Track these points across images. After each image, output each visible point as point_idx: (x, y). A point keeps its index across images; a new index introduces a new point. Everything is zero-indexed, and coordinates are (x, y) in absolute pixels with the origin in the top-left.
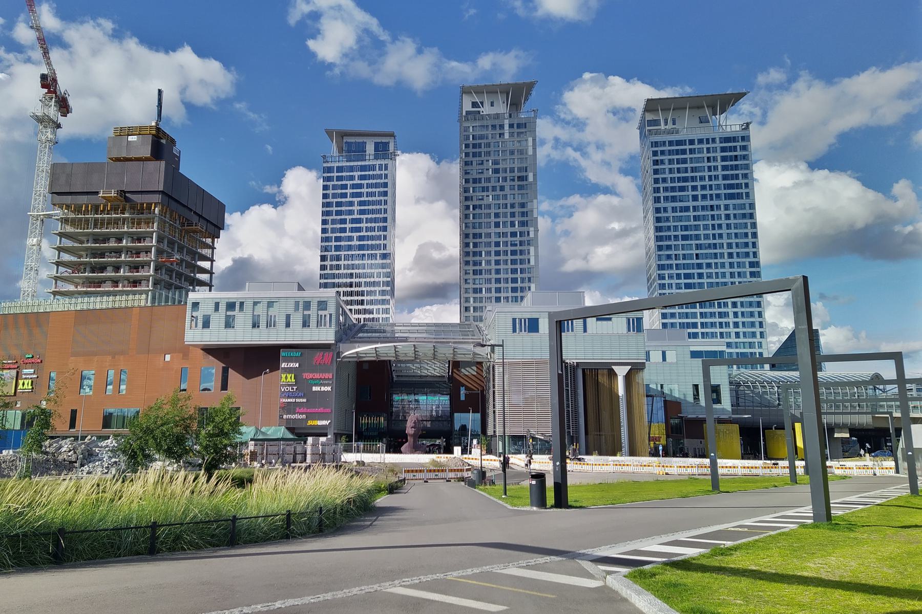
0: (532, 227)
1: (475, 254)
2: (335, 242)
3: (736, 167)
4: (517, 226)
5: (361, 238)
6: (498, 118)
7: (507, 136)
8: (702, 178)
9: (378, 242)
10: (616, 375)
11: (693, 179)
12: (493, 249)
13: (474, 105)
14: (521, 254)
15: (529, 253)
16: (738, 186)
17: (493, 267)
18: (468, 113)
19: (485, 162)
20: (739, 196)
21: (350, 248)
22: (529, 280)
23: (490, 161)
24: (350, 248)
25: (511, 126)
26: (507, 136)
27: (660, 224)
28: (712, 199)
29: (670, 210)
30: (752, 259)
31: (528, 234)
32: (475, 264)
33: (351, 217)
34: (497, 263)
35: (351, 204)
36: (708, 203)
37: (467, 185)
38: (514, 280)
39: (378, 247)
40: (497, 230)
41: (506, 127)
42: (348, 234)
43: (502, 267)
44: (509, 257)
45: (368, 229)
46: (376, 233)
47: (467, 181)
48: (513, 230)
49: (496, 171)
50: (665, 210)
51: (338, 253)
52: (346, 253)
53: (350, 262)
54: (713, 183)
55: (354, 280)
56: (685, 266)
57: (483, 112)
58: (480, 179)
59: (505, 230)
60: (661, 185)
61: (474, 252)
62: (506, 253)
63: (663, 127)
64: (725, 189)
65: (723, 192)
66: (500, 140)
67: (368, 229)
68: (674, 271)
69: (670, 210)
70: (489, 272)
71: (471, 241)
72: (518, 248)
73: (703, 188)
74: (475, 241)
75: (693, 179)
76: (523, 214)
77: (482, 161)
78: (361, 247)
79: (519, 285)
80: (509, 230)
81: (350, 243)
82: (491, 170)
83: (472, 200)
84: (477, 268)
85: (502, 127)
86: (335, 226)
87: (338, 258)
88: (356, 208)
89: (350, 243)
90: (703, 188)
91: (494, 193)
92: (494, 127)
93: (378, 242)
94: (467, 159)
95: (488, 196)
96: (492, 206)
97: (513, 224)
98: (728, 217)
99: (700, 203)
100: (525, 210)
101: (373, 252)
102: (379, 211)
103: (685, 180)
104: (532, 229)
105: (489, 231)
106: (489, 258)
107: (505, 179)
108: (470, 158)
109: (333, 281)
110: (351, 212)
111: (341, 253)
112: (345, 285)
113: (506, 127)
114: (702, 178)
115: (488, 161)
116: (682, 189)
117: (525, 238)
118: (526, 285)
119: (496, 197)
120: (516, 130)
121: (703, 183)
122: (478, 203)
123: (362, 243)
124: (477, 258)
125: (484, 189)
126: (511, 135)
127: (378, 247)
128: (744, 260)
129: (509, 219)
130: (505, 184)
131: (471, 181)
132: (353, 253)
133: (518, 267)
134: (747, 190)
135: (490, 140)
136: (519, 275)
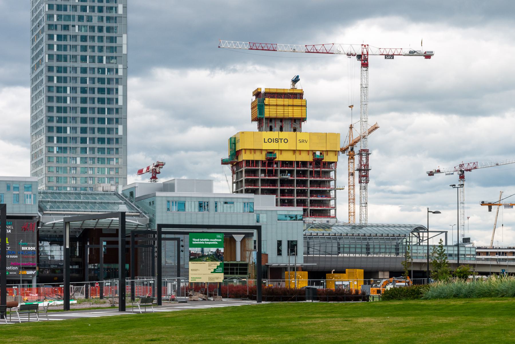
0: (121, 64)
1: (59, 90)
10: (235, 241)
12: (79, 85)
14: (109, 93)
22: (117, 122)
31: (117, 72)
34: (84, 100)
38: (101, 121)
43: (88, 105)
44: (97, 95)
48: (101, 65)
62: (93, 90)
70: (75, 109)
74: (60, 75)
76: (112, 49)
79: (106, 125)
80: (96, 65)
83: (56, 29)
95: (74, 26)
97: (101, 60)
100: (113, 45)
104: (120, 66)
105: (75, 65)
106: (74, 95)
117: (113, 76)
118: (114, 126)
122: (63, 33)
129: (97, 54)
130: (92, 14)
131: (55, 7)
133: (106, 106)
136: (106, 116)
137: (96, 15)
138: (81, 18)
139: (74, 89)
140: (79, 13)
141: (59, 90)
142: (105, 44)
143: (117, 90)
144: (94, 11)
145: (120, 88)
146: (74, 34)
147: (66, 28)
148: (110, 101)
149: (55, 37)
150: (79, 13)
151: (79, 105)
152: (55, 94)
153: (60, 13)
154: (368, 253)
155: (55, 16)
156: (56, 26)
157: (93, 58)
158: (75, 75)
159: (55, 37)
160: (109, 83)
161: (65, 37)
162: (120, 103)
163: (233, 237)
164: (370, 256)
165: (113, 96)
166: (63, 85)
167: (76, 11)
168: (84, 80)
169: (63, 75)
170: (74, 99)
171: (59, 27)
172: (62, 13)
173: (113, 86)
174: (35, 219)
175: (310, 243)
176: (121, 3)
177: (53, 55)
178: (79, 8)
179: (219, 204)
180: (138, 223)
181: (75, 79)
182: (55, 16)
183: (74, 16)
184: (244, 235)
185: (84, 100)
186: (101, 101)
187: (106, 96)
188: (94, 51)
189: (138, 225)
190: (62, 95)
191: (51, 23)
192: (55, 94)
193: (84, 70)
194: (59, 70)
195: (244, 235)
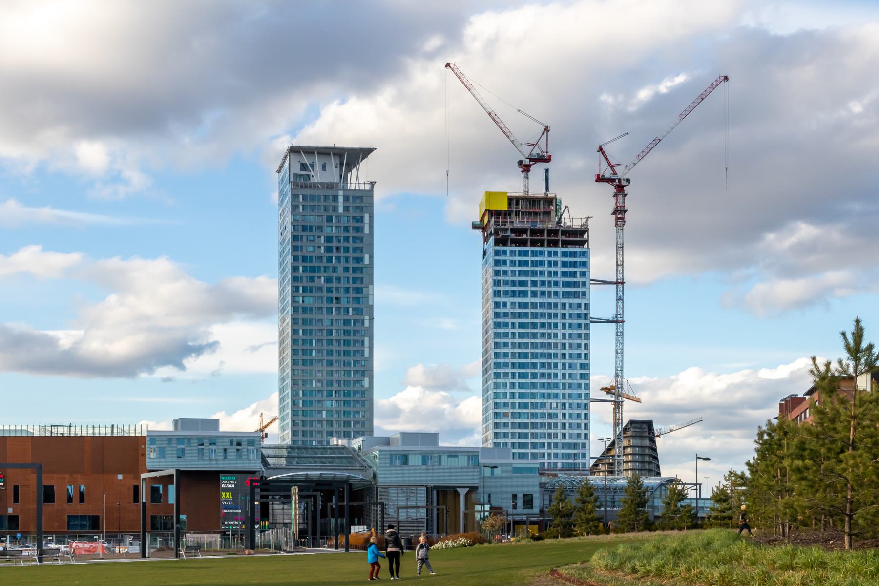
3: (575, 264)
4: (350, 314)
6: (332, 188)
8: (542, 273)
11: (534, 273)
12: (325, 337)
13: (304, 167)
16: (576, 284)
17: (325, 358)
18: (296, 175)
19: (316, 237)
20: (576, 295)
23: (323, 238)
25: (346, 198)
27: (498, 320)
28: (550, 297)
29: (509, 305)
30: (583, 361)
31: (363, 323)
32: (304, 352)
36: (546, 300)
37: (296, 264)
41: (341, 199)
43: (334, 358)
47: (296, 259)
48: (346, 318)
49: (328, 250)
50: (505, 304)
54: (553, 279)
56: (521, 366)
58: (311, 257)
59: (338, 317)
60: (502, 278)
61: (303, 340)
64: (563, 286)
65: (560, 289)
68: (509, 370)
69: (509, 305)
73: (543, 283)
74: (305, 327)
75: (534, 273)
76: (357, 300)
82: (322, 248)
84: (307, 358)
85: (335, 198)
90: (543, 283)
91: (326, 275)
92: (326, 198)
94: (296, 234)
95: (319, 278)
96: (324, 290)
98: (564, 316)
99: (538, 300)
103: (526, 273)
104: (367, 318)
107: (338, 259)
108: (300, 233)
113: (341, 199)
114: (542, 273)
115: (319, 237)
116: (523, 283)
119: (328, 280)
121: (542, 279)
126: (346, 209)
128: (575, 361)
131: (300, 258)
134: (583, 290)
139: (319, 341)
141: (304, 342)
143: (363, 342)
144: (339, 262)
145: (366, 340)
147: (312, 279)
149: (301, 289)
150: (325, 264)
152: (300, 347)
153: (305, 264)
154: (614, 507)
155: (301, 268)
156: (301, 277)
157: (338, 309)
159: (301, 289)
160: (355, 335)
161: (311, 289)
163: (457, 490)
164: (615, 509)
165: (358, 347)
167: (322, 262)
168: (330, 333)
169: (307, 327)
170: (319, 351)
171: (305, 279)
172: (307, 264)
174: (257, 474)
175: (553, 497)
176: (367, 254)
177: (298, 308)
178: (324, 259)
179: (443, 457)
180: (361, 477)
182: (301, 268)
183: (319, 267)
184: (468, 489)
185: (330, 353)
187: (352, 348)
189: (363, 479)
190: (307, 347)
191: (296, 274)
194: (304, 322)
195: (468, 489)
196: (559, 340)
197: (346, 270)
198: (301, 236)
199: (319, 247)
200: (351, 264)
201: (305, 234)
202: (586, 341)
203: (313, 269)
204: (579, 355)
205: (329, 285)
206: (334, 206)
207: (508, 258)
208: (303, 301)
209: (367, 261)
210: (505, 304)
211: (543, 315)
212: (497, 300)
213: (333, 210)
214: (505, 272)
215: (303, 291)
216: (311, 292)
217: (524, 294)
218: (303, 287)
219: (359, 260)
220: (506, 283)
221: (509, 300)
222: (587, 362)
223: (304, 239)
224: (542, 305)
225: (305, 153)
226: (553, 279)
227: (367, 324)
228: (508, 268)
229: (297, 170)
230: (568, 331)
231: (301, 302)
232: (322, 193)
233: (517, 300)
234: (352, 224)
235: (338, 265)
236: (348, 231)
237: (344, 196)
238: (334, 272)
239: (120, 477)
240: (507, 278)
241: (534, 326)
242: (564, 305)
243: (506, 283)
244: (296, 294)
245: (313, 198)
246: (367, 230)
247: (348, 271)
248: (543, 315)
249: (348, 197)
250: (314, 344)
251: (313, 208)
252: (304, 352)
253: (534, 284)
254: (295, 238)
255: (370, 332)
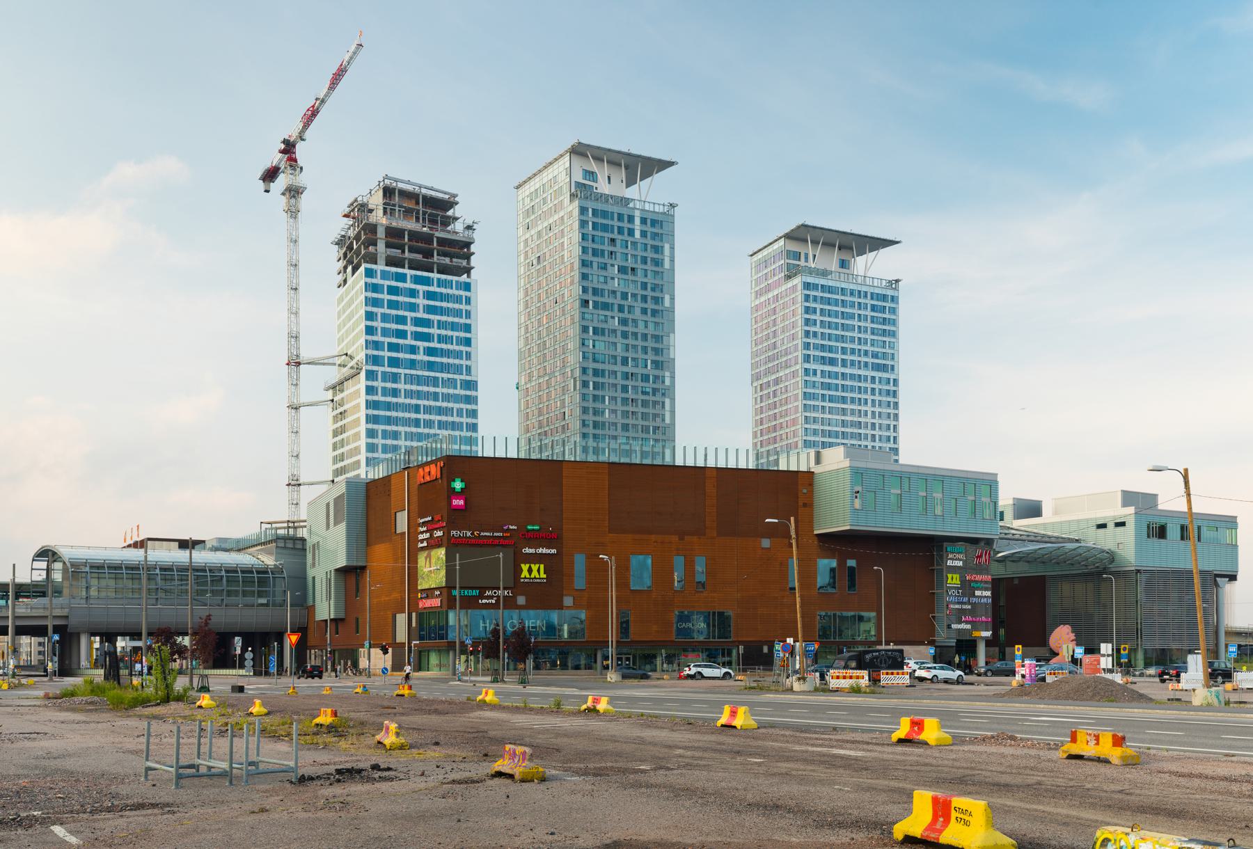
1: (595, 398)
2: (388, 351)
5: (430, 352)
7: (637, 234)
8: (852, 340)
9: (457, 361)
11: (842, 339)
12: (619, 395)
13: (590, 175)
15: (663, 407)
17: (620, 420)
20: (883, 368)
21: (412, 364)
24: (412, 364)
25: (644, 221)
26: (637, 234)
32: (596, 412)
33: (413, 315)
34: (625, 414)
35: (413, 293)
36: (856, 371)
37: (586, 297)
39: (458, 370)
40: (625, 369)
41: (637, 221)
42: (409, 341)
44: (640, 409)
45: (442, 339)
46: (454, 347)
47: (585, 290)
48: (645, 371)
50: (815, 372)
51: (394, 370)
52: (408, 371)
53: (414, 387)
54: (863, 348)
55: (421, 416)
57: (596, 188)
59: (634, 370)
60: (812, 341)
61: (594, 396)
63: (802, 263)
66: (630, 239)
67: (442, 339)
71: (591, 381)
72: (651, 398)
73: (853, 351)
74: (596, 379)
75: (842, 339)
76: (657, 351)
77: (606, 264)
78: (430, 366)
81: (413, 357)
85: (631, 219)
86: (387, 325)
87: (395, 378)
88: (421, 301)
89: (413, 357)
90: (853, 351)
91: (621, 315)
92: (620, 218)
93: (457, 361)
95: (613, 317)
99: (848, 371)
100: (660, 346)
101: (451, 376)
102: (458, 313)
104: (667, 374)
105: (616, 368)
108: (589, 257)
109: (388, 413)
110: (413, 307)
111: (400, 371)
112: (407, 422)
113: (637, 221)
114: (852, 340)
116: (830, 349)
119: (624, 322)
120: (649, 229)
123: (432, 359)
124: (599, 405)
125: (606, 306)
126: (644, 234)
127: (458, 370)
129: (640, 355)
130: (635, 304)
131: (590, 291)
132: (420, 373)
133: (651, 424)
134: (892, 363)
135: (615, 236)
137: (639, 305)
138: (621, 309)
139: (613, 399)
140: (618, 301)
142: (650, 344)
144: (636, 301)
145: (667, 401)
146: (613, 328)
148: (655, 416)
149: (591, 329)
150: (618, 301)
151: (620, 420)
152: (591, 404)
158: (615, 382)
159: (591, 329)
161: (603, 330)
162: (668, 420)
166: (599, 393)
168: (625, 389)
169: (600, 380)
170: (614, 412)
173: (658, 398)
181: (615, 385)
183: (612, 304)
186: (645, 416)
187: (650, 411)
188: (637, 352)
190: (599, 405)
192: (591, 404)
193: (626, 376)
194: (596, 373)
196: (869, 420)
197: (644, 311)
198: (591, 262)
199: (613, 278)
200: (650, 305)
201: (595, 259)
202: (895, 423)
203: (606, 306)
204: (888, 440)
205: (625, 329)
206: (629, 229)
207: (818, 317)
208: (594, 346)
209: (667, 303)
210: (815, 372)
211: (852, 389)
212: (807, 366)
213: (629, 234)
214: (815, 334)
215: (594, 333)
216: (603, 334)
217: (832, 362)
218: (594, 328)
219: (657, 300)
220: (816, 347)
221: (819, 367)
222: (896, 446)
223: (595, 265)
224: (852, 377)
225: (594, 158)
226: (863, 348)
227: (667, 382)
228: (817, 329)
229: (578, 177)
230: (877, 410)
231: (591, 347)
232: (616, 209)
233: (827, 368)
234: (650, 254)
235: (635, 304)
236: (646, 263)
237: (641, 218)
238: (629, 312)
239: (766, 543)
240: (817, 342)
241: (844, 400)
242: (873, 378)
243: (816, 347)
244: (585, 336)
245: (605, 214)
246: (667, 265)
247: (646, 313)
248: (852, 389)
249: (646, 219)
250: (607, 403)
251: (605, 228)
252: (596, 412)
253: (844, 351)
254: (584, 263)
255: (669, 392)
